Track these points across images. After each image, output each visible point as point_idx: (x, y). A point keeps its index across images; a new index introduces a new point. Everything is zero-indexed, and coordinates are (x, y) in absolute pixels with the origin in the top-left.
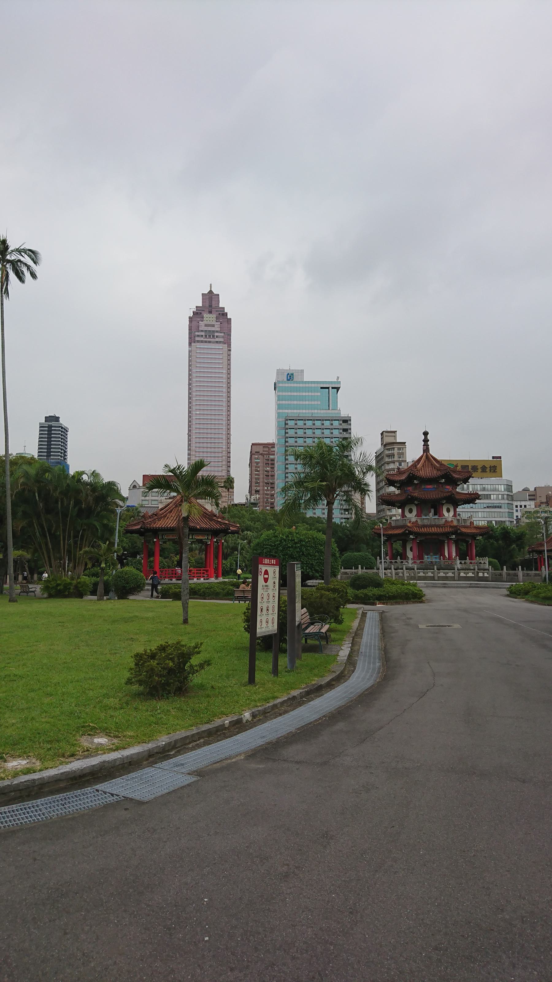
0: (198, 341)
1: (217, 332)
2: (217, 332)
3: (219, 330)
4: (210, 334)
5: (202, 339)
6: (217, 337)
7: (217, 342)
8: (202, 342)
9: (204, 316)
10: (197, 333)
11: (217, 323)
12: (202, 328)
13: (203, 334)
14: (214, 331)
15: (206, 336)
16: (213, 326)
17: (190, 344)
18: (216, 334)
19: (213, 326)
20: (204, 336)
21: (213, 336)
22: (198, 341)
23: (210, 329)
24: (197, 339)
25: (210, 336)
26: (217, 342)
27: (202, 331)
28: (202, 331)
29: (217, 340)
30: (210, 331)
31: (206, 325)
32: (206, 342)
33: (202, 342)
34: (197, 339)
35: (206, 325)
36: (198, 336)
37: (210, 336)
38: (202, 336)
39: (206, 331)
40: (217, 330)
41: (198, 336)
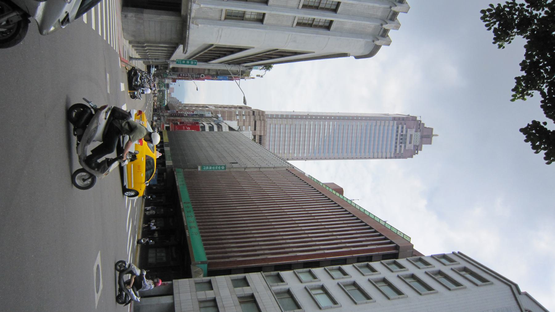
0: (398, 128)
1: (405, 146)
2: (405, 146)
3: (406, 149)
4: (403, 139)
5: (400, 132)
6: (401, 146)
7: (396, 147)
8: (397, 132)
9: (418, 133)
10: (405, 126)
11: (412, 146)
12: (410, 132)
13: (404, 133)
14: (405, 143)
15: (402, 135)
16: (410, 143)
17: (394, 119)
18: (403, 145)
19: (410, 143)
20: (402, 133)
21: (401, 143)
22: (398, 128)
23: (408, 139)
24: (400, 126)
25: (402, 139)
26: (396, 147)
27: (407, 132)
28: (407, 132)
29: (398, 147)
30: (406, 139)
31: (411, 135)
32: (397, 135)
33: (397, 132)
34: (400, 126)
35: (411, 135)
36: (402, 128)
37: (402, 139)
38: (402, 132)
39: (406, 135)
40: (407, 146)
41: (402, 128)
